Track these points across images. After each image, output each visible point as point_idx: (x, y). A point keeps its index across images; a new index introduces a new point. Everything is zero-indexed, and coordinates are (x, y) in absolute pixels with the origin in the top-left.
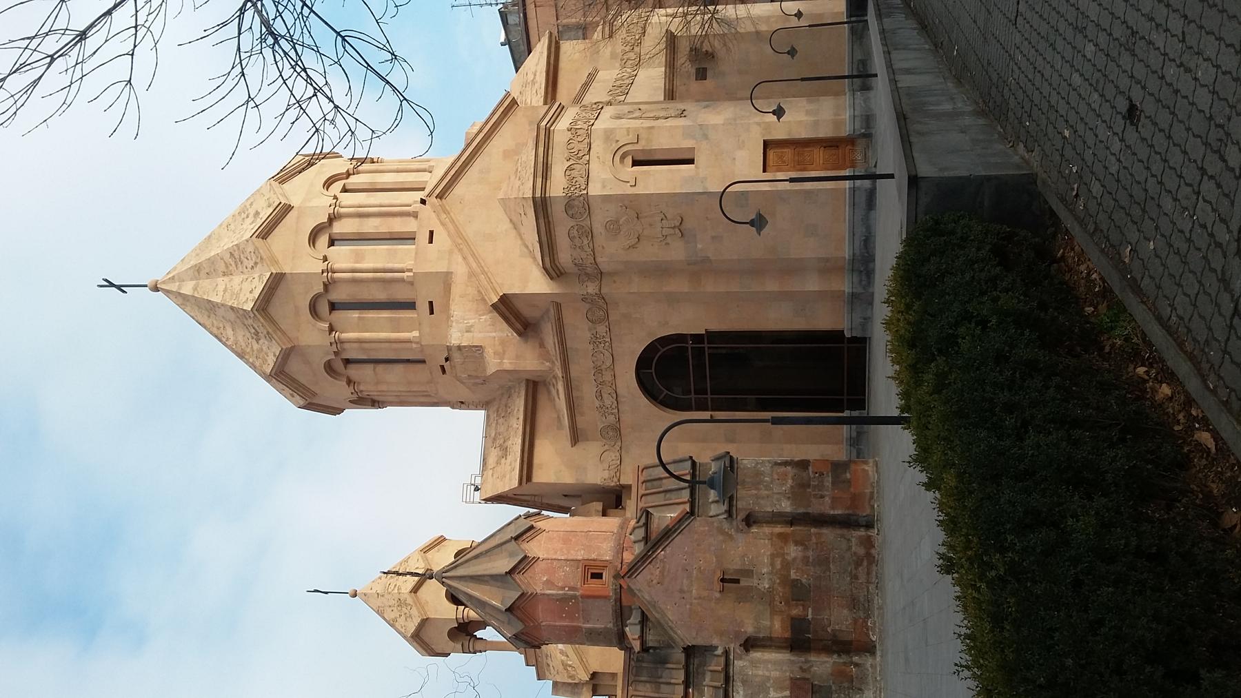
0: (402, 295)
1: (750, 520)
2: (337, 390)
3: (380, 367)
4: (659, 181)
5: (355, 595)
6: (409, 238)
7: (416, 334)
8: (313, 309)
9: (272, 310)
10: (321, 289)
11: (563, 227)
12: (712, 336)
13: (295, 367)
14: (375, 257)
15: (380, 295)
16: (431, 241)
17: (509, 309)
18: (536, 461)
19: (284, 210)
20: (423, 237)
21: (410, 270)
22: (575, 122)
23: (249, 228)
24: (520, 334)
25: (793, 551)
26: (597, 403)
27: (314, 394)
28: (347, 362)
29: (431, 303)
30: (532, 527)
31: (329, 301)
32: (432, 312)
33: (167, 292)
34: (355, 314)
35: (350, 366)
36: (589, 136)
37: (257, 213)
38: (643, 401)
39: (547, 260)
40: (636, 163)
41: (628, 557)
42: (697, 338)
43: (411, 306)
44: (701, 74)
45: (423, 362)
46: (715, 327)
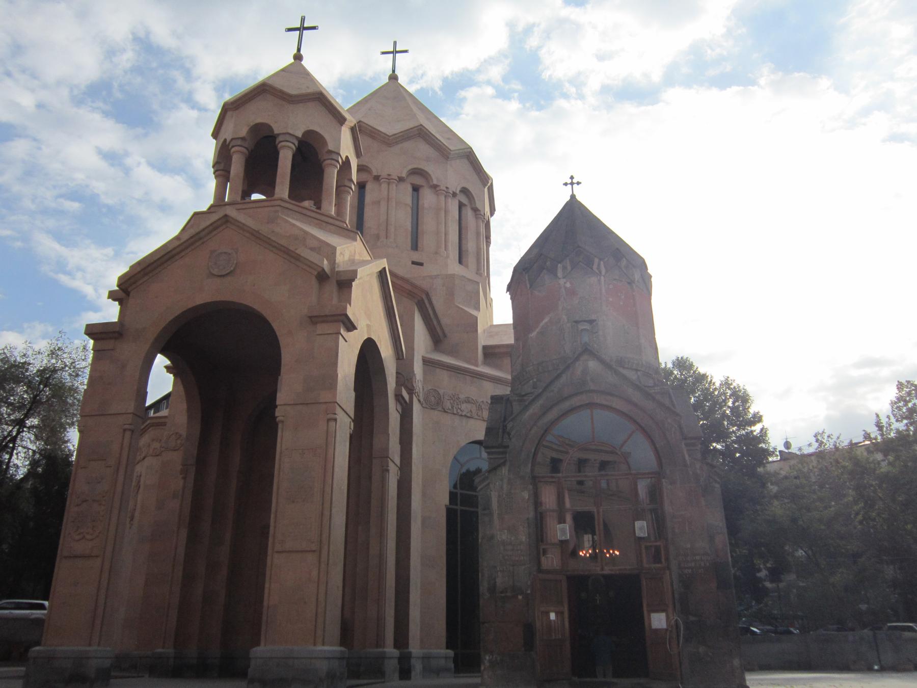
5: (298, 57)
8: (465, 191)
9: (466, 161)
13: (422, 149)
15: (470, 245)
26: (462, 397)
35: (410, 189)
45: (415, 247)
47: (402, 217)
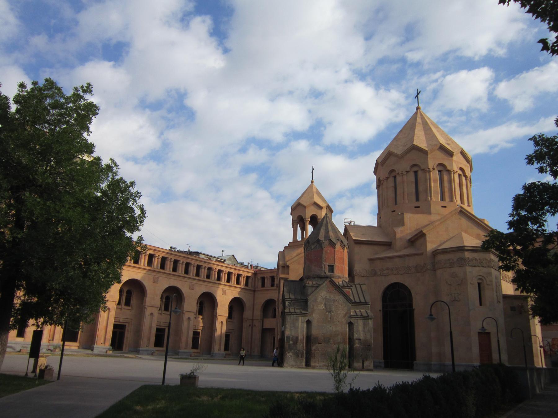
0: (421, 196)
1: (350, 324)
2: (384, 174)
3: (394, 189)
4: (473, 293)
5: (312, 182)
6: (443, 199)
7: (407, 201)
10: (422, 168)
11: (454, 257)
12: (412, 311)
14: (435, 187)
15: (421, 189)
16: (442, 207)
17: (419, 237)
18: (362, 246)
19: (450, 154)
20: (444, 204)
21: (431, 199)
22: (493, 261)
23: (442, 141)
24: (409, 240)
25: (339, 338)
27: (382, 166)
28: (395, 177)
29: (419, 207)
30: (345, 246)
31: (418, 172)
32: (415, 207)
33: (416, 113)
34: (413, 179)
35: (393, 179)
36: (489, 267)
37: (449, 144)
38: (386, 285)
39: (440, 251)
40: (479, 284)
41: (336, 280)
42: (411, 305)
43: (417, 199)
44: (513, 309)
46: (416, 312)
47: (391, 194)
